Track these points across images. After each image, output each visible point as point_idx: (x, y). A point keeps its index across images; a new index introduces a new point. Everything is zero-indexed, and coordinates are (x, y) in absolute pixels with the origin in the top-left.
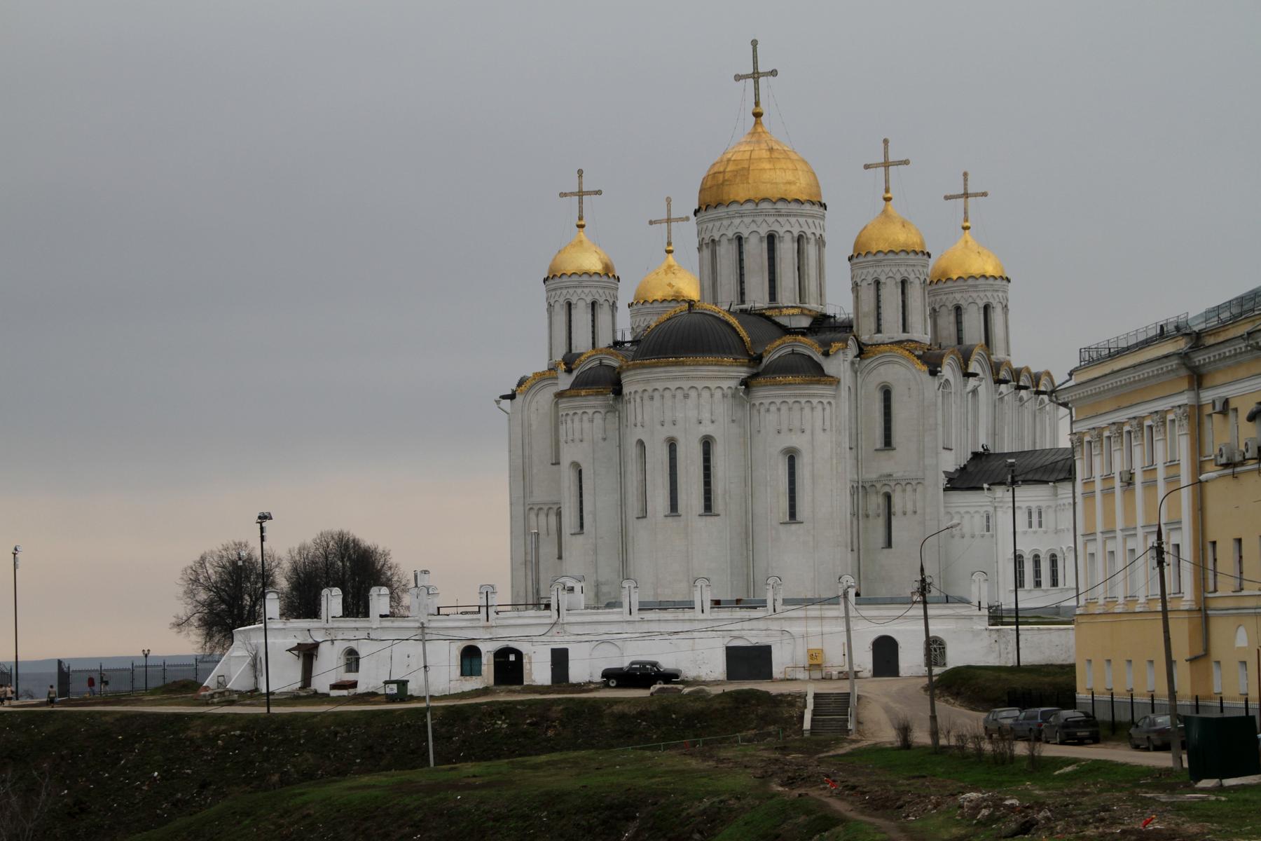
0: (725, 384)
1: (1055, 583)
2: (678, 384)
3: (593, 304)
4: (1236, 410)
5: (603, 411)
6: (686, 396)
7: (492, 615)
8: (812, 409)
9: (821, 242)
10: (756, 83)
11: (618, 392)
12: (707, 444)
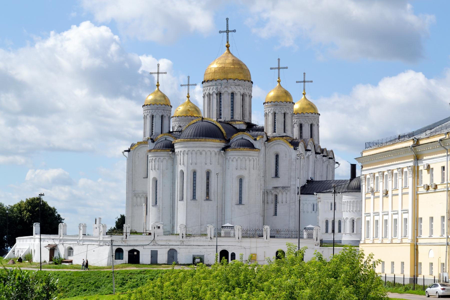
1: (340, 231)
2: (198, 149)
3: (162, 116)
4: (432, 169)
5: (167, 158)
6: (201, 154)
8: (250, 160)
9: (250, 96)
10: (228, 34)
11: (173, 151)
12: (208, 174)
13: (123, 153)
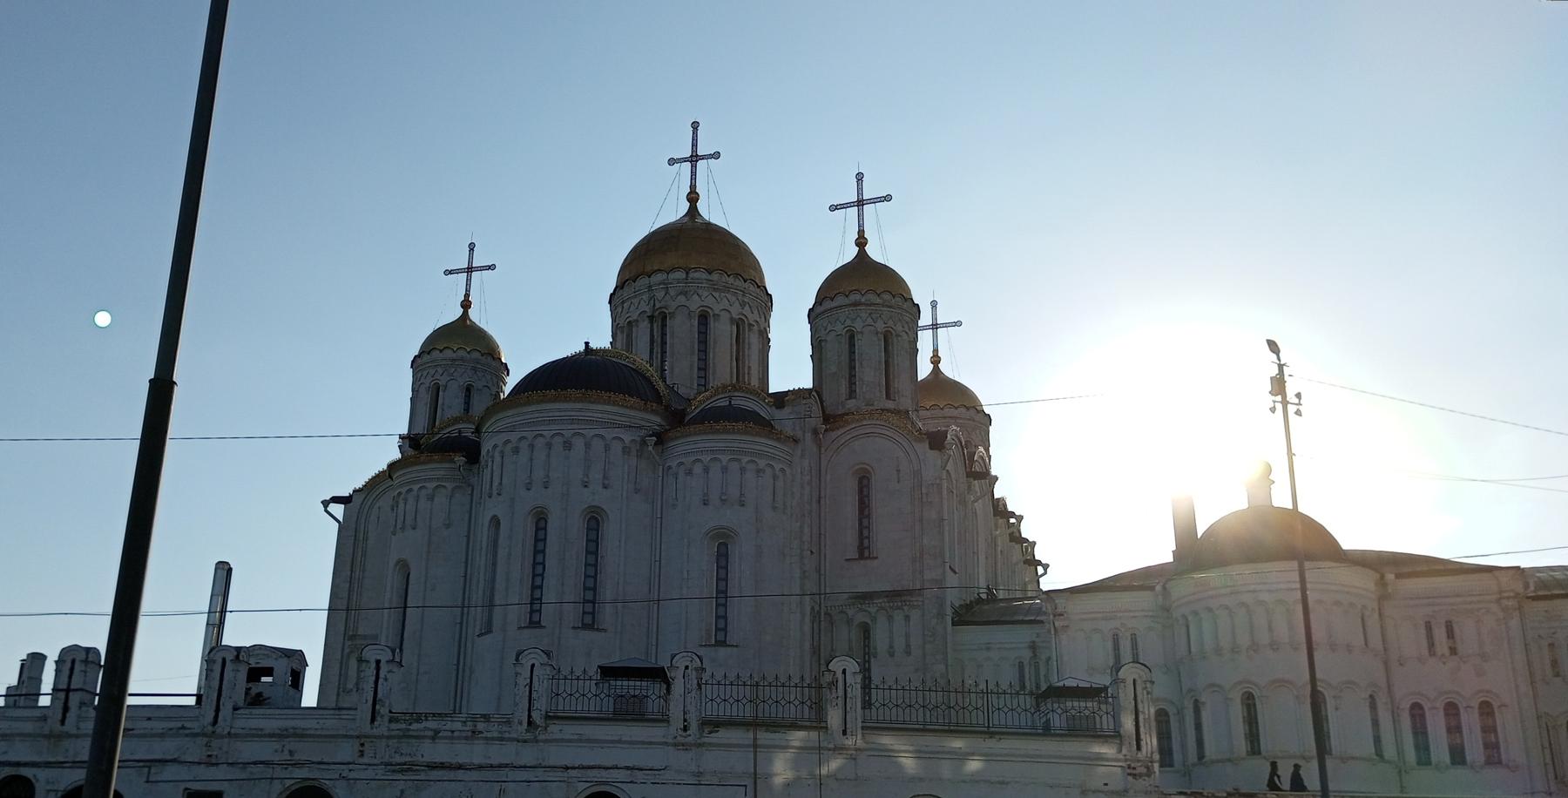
0: (627, 437)
6: (568, 445)
7: (71, 716)
8: (758, 471)
12: (594, 521)
13: (326, 504)
